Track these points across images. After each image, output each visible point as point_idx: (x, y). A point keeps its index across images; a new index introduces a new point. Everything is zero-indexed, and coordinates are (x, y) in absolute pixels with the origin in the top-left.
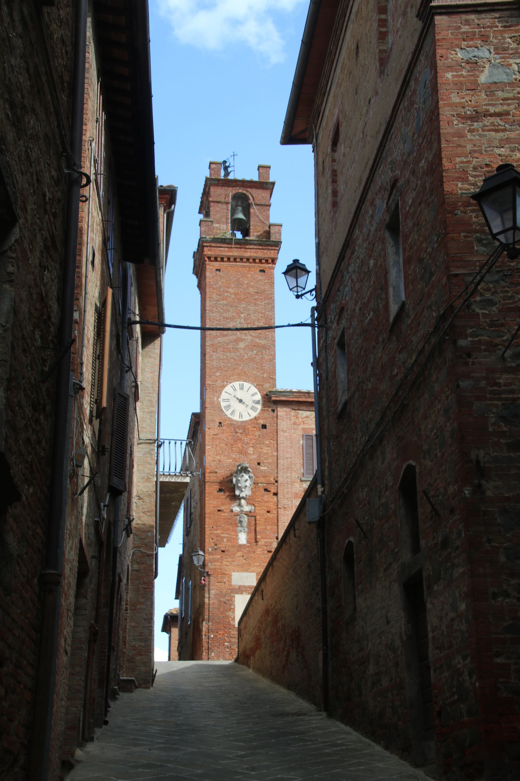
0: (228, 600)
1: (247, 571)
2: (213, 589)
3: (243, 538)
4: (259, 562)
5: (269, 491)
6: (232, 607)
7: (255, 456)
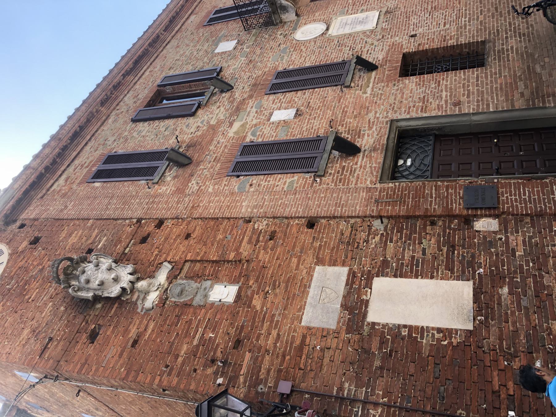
0: (383, 342)
1: (305, 287)
2: (341, 389)
3: (223, 293)
5: (149, 235)
6: (405, 332)
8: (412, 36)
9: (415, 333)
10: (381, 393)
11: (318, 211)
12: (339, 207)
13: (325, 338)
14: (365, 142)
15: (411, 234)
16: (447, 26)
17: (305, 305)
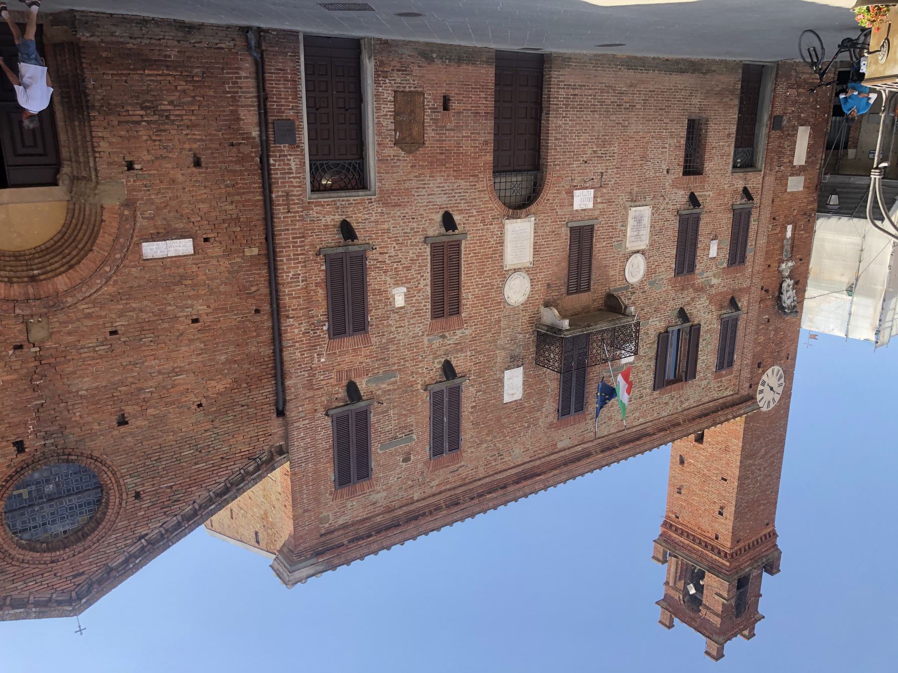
7: (770, 328)
8: (668, 172)
14: (740, 185)
16: (667, 146)
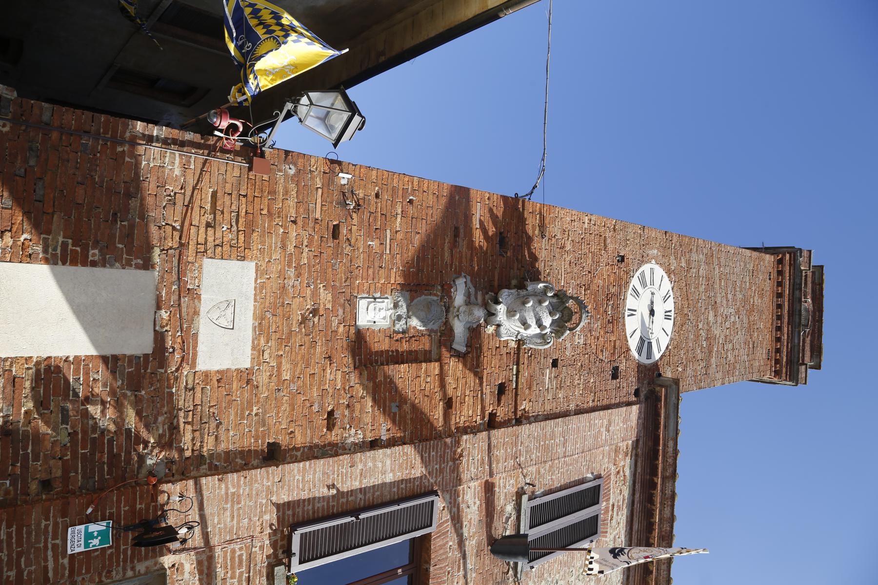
1: (261, 328)
4: (292, 381)
6: (94, 253)
9: (77, 251)
10: (127, 159)
11: (268, 479)
12: (233, 494)
13: (217, 242)
15: (93, 454)
17: (255, 295)
